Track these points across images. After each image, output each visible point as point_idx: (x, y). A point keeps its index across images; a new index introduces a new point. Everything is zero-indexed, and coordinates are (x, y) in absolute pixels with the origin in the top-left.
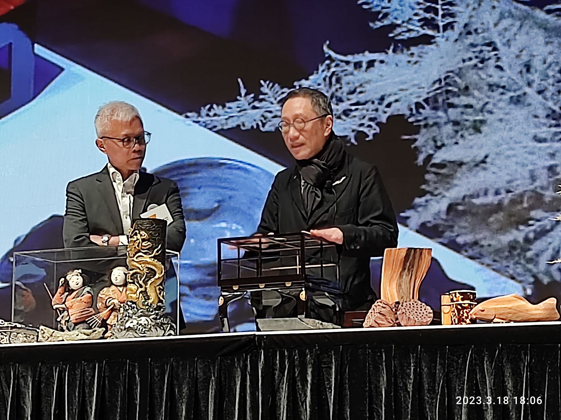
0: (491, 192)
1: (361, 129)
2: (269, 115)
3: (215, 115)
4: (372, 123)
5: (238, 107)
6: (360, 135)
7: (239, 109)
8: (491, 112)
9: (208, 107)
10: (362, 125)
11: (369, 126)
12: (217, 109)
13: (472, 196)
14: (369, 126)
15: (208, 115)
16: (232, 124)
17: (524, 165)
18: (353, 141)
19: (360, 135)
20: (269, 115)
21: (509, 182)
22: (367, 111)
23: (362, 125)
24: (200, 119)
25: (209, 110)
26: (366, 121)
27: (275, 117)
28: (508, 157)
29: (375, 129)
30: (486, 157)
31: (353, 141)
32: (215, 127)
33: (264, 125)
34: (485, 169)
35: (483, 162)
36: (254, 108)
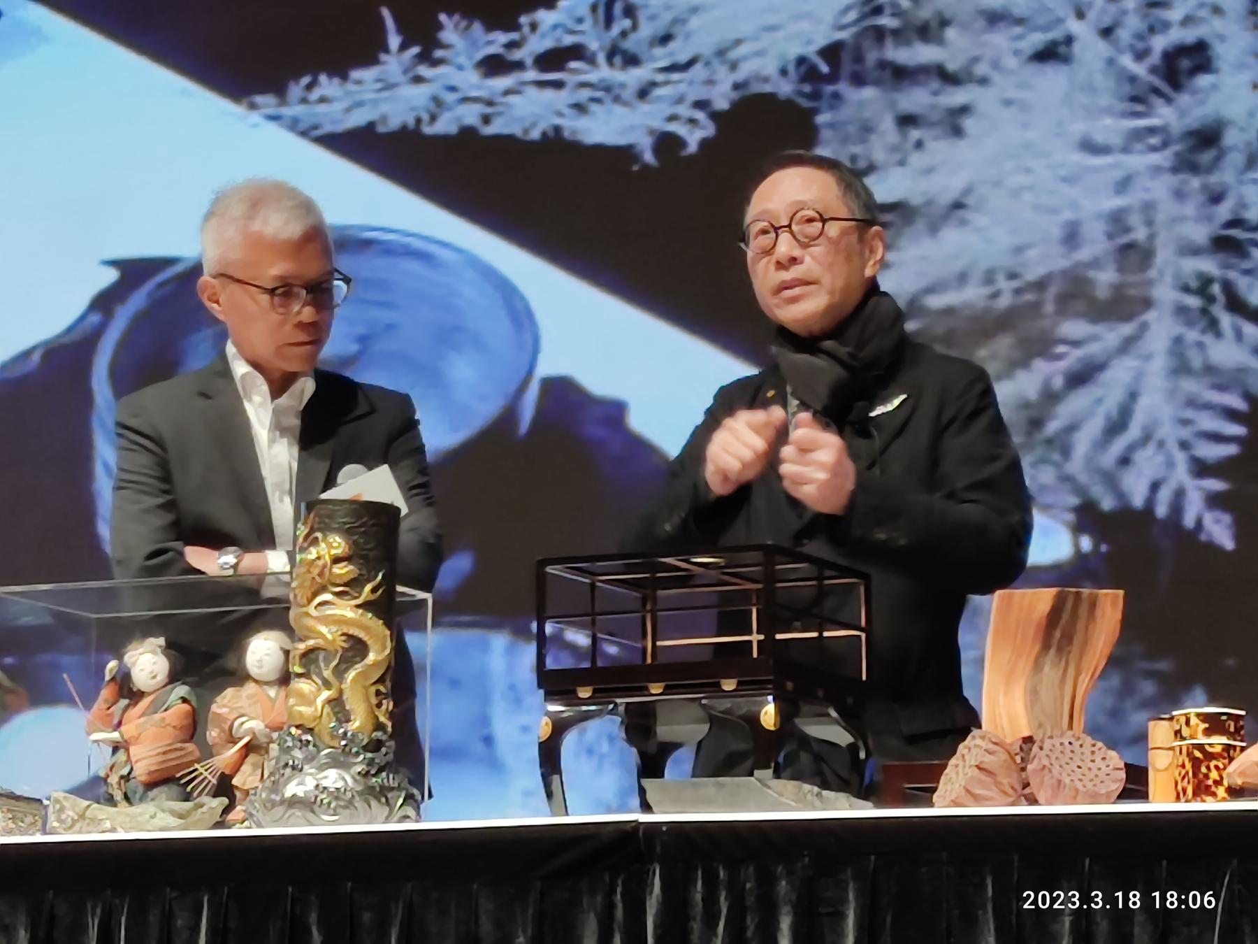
0: (976, 277)
1: (673, 127)
2: (450, 97)
3: (323, 100)
4: (700, 116)
5: (378, 80)
6: (667, 143)
7: (379, 85)
8: (983, 81)
9: (306, 80)
10: (673, 118)
11: (692, 121)
12: (327, 85)
13: (930, 290)
14: (692, 121)
15: (304, 101)
16: (357, 119)
17: (1053, 211)
18: (649, 157)
19: (667, 143)
20: (450, 97)
21: (1019, 250)
22: (691, 83)
23: (673, 118)
24: (287, 111)
25: (310, 87)
26: (684, 111)
27: (466, 100)
28: (1016, 193)
29: (703, 128)
30: (968, 191)
31: (649, 157)
32: (316, 127)
33: (433, 118)
34: (963, 223)
35: (958, 205)
36: (418, 80)
